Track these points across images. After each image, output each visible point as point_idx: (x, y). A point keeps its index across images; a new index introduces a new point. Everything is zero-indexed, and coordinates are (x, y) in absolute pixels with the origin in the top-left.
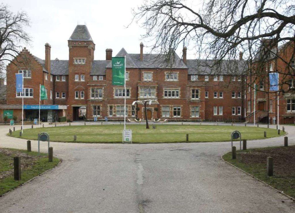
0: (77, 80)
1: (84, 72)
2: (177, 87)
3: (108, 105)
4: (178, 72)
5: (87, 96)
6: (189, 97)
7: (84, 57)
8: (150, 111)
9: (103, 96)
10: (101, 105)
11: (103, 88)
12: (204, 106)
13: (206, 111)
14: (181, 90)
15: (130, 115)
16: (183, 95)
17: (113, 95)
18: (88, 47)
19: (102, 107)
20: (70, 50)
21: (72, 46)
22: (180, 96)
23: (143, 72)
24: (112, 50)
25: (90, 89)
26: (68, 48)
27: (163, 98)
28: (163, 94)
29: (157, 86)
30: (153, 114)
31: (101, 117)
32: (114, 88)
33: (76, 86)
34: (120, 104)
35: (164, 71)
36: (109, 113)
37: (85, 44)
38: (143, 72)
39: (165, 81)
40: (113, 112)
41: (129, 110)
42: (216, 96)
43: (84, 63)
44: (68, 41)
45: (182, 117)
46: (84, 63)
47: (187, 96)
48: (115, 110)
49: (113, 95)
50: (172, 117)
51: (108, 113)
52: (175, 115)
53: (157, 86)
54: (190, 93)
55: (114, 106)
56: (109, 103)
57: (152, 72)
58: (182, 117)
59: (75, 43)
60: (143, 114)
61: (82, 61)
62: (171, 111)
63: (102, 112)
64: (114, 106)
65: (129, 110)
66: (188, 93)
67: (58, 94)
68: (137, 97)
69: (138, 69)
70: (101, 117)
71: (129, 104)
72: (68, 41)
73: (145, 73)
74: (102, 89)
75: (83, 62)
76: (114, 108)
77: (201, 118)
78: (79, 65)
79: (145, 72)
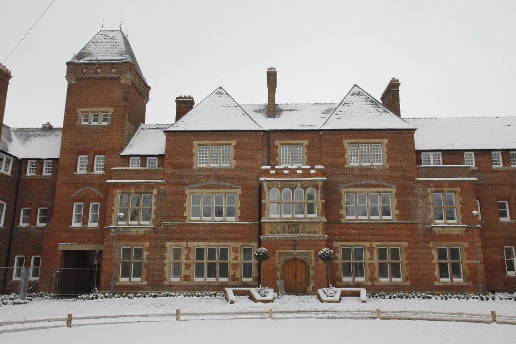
0: (81, 171)
1: (102, 148)
2: (384, 187)
3: (169, 244)
4: (386, 141)
5: (104, 217)
6: (425, 216)
7: (108, 106)
8: (305, 263)
9: (153, 216)
10: (147, 244)
11: (155, 192)
12: (478, 245)
13: (486, 261)
14: (399, 195)
15: (238, 276)
16: (405, 209)
17: (185, 214)
18: (119, 78)
19: (147, 250)
20: (70, 87)
21: (77, 79)
22: (397, 212)
23: (277, 143)
24: (192, 98)
25: (114, 196)
26: (65, 84)
27: (343, 221)
28: (341, 207)
29: (325, 178)
30: (312, 273)
31: (145, 283)
32: (187, 192)
33: (77, 189)
34: (204, 240)
35: (342, 139)
36: (169, 269)
37: (114, 70)
38: (277, 143)
39: (346, 166)
40: (183, 267)
41: (235, 262)
42: (504, 215)
43: (106, 123)
44: (68, 64)
45: (408, 283)
46: (106, 123)
47: (419, 212)
48: (187, 261)
49: (185, 214)
50: (376, 283)
51: (166, 269)
52: (383, 274)
53: (325, 181)
54: (430, 204)
55: (186, 248)
56: (172, 237)
57: (306, 142)
58: (408, 283)
59: (85, 70)
60: (278, 274)
61: (101, 117)
62: (371, 262)
63: (147, 266)
64: (186, 248)
65: (235, 262)
66: (421, 203)
67: (28, 212)
68: (260, 218)
69: (262, 133)
70: (145, 283)
71: (232, 242)
72: (68, 64)
73: (282, 144)
74: (151, 193)
75: (104, 120)
76: (185, 252)
77: (471, 284)
78: (90, 129)
79: (282, 142)
